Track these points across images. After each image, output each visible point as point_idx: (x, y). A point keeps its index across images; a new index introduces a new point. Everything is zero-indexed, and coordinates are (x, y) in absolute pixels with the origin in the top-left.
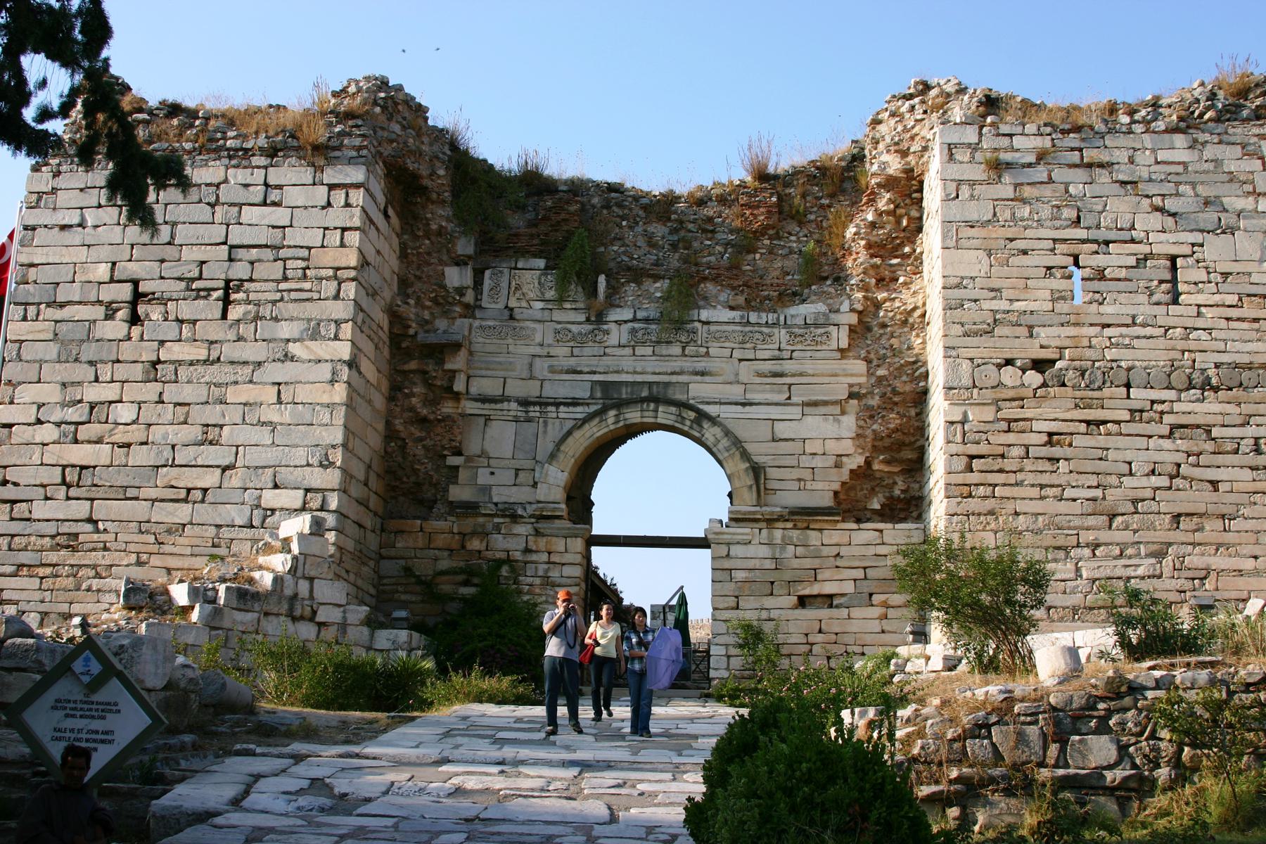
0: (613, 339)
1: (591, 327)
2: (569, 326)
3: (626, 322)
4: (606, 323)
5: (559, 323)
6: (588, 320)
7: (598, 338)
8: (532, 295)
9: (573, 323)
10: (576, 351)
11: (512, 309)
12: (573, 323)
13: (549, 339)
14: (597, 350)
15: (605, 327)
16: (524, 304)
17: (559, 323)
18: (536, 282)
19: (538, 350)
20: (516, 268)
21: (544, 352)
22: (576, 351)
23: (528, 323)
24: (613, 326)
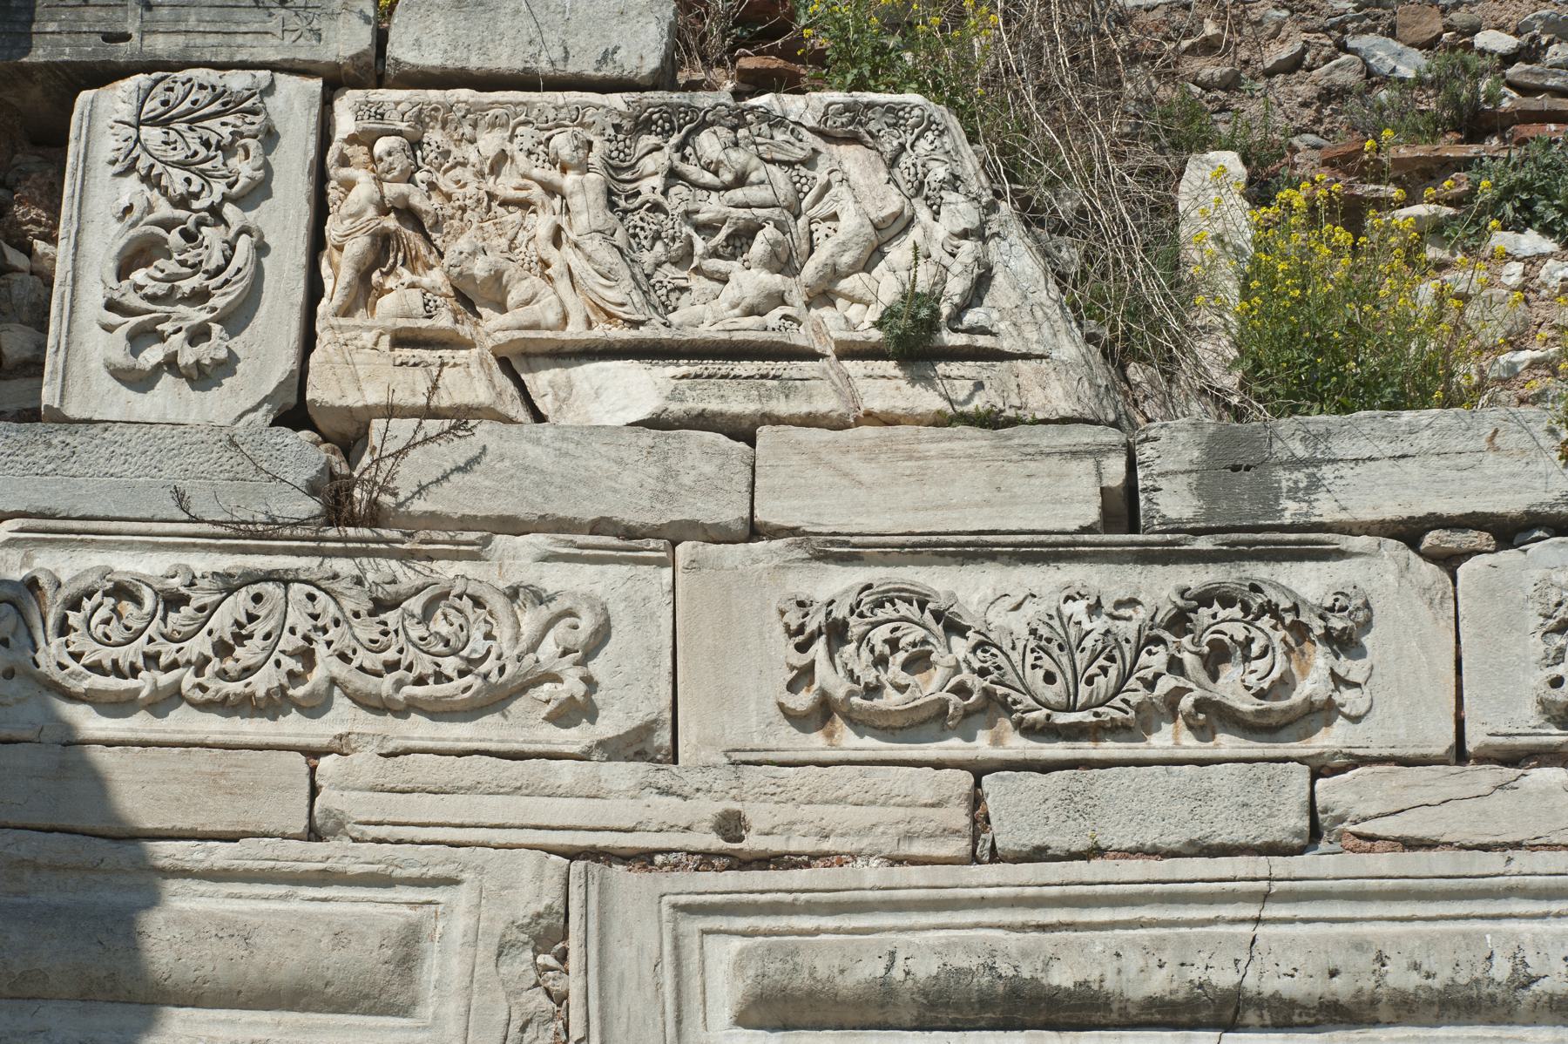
0: (1398, 696)
1: (1161, 587)
2: (939, 581)
3: (1509, 532)
4: (1311, 543)
5: (837, 550)
6: (1122, 508)
7: (1234, 686)
8: (539, 306)
9: (973, 550)
10: (1018, 808)
11: (348, 434)
12: (973, 550)
13: (740, 697)
14: (1251, 794)
15: (1308, 582)
16: (468, 380)
17: (837, 550)
18: (584, 190)
19: (623, 802)
20: (374, 69)
21: (679, 814)
22: (1018, 808)
23: (518, 558)
24: (1382, 573)
